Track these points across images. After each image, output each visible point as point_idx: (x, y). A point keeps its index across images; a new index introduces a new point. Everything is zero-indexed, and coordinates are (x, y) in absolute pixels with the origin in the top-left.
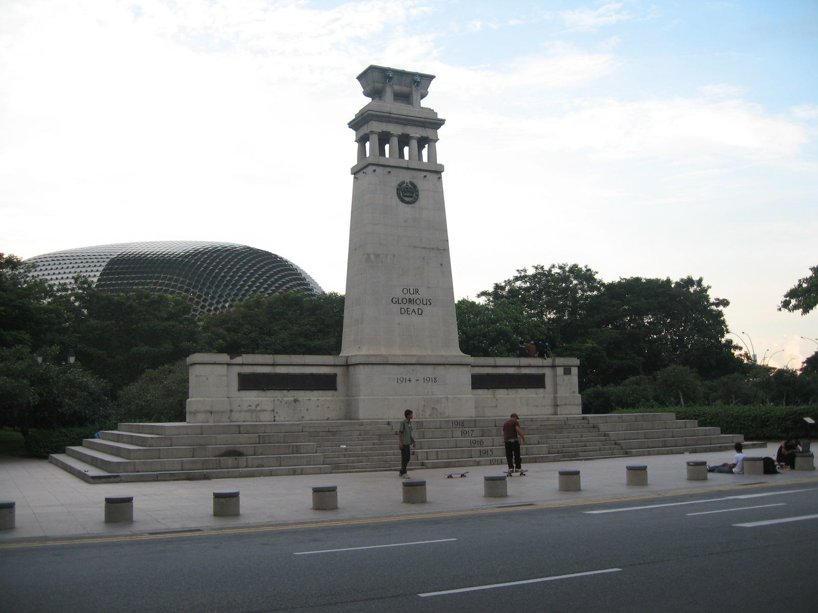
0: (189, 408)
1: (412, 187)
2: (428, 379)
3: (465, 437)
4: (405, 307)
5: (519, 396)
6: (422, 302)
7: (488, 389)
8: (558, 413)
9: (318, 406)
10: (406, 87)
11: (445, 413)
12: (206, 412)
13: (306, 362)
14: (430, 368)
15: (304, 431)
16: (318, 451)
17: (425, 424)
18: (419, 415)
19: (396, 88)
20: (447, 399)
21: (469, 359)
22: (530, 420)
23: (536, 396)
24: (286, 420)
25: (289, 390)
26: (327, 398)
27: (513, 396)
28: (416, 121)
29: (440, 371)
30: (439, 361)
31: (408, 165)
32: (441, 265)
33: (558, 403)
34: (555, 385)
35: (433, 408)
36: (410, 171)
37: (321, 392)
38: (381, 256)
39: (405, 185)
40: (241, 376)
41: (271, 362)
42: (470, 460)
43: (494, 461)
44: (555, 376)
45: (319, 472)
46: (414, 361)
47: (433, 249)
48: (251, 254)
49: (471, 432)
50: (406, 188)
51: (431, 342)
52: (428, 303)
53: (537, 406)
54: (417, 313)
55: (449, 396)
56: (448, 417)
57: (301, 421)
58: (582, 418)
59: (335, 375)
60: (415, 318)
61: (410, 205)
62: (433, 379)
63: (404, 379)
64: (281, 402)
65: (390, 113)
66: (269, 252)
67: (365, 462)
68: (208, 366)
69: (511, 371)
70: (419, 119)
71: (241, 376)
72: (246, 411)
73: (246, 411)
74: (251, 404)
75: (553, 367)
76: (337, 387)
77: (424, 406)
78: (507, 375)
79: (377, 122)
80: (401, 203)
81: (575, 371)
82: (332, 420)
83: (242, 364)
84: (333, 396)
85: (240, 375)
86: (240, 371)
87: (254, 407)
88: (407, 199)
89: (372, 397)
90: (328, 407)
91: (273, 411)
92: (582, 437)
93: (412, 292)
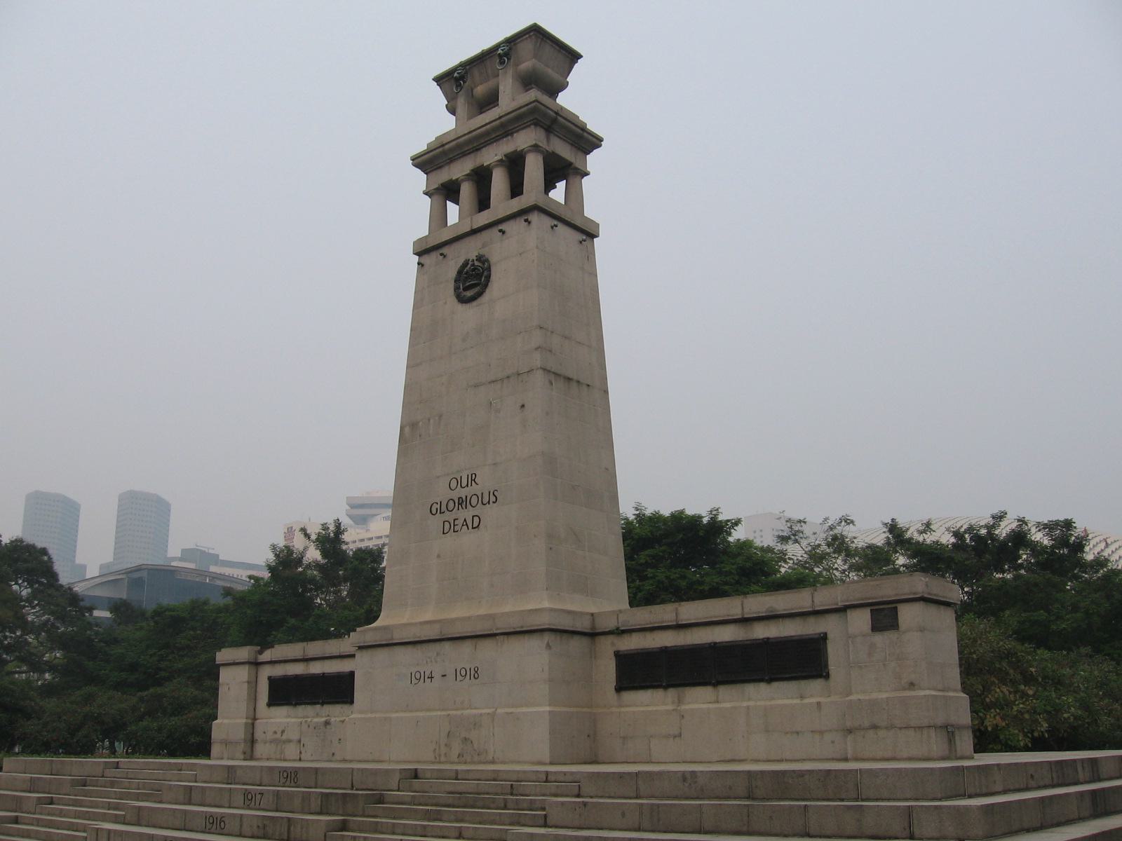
0: (215, 734)
4: (449, 516)
5: (745, 704)
11: (486, 752)
14: (467, 647)
18: (440, 756)
22: (453, 775)
25: (322, 704)
28: (487, 133)
29: (487, 650)
30: (480, 628)
32: (523, 406)
35: (465, 739)
38: (421, 423)
40: (273, 682)
47: (508, 377)
49: (258, 797)
53: (798, 733)
56: (493, 762)
60: (467, 539)
61: (474, 303)
62: (473, 672)
63: (422, 674)
65: (443, 145)
69: (725, 635)
70: (488, 126)
71: (273, 682)
73: (271, 742)
78: (714, 647)
87: (278, 735)
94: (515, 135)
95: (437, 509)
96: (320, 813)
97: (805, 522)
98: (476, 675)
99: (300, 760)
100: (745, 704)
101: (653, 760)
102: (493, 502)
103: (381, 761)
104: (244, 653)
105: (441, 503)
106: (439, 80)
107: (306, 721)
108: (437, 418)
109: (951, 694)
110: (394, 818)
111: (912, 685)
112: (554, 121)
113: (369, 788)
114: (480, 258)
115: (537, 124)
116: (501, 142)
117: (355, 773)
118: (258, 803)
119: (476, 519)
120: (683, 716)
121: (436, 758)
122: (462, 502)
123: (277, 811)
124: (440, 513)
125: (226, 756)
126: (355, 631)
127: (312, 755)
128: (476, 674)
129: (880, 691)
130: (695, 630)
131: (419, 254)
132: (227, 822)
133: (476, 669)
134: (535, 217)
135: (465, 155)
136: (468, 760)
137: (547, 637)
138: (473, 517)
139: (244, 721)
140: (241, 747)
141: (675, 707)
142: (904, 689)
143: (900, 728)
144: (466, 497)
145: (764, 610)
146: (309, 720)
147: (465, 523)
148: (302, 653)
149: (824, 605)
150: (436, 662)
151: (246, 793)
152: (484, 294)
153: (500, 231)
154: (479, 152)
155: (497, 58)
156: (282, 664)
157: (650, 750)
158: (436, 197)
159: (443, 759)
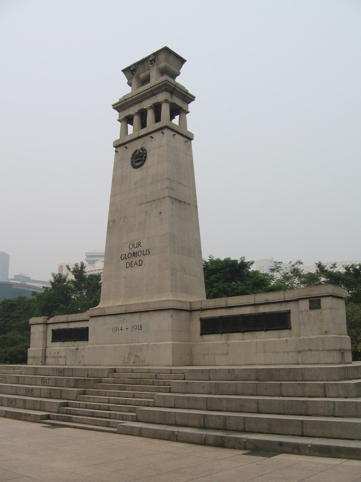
0: (29, 354)
2: (135, 328)
4: (129, 260)
5: (255, 340)
7: (222, 333)
13: (83, 318)
14: (137, 316)
18: (125, 363)
23: (278, 339)
25: (75, 341)
28: (145, 94)
32: (161, 213)
36: (142, 138)
38: (117, 220)
40: (54, 332)
41: (65, 320)
47: (154, 200)
49: (48, 380)
52: (148, 253)
56: (148, 365)
60: (137, 270)
61: (140, 168)
62: (139, 327)
64: (69, 350)
65: (126, 100)
70: (146, 91)
71: (54, 332)
73: (53, 357)
78: (243, 316)
80: (134, 169)
87: (56, 355)
88: (137, 164)
94: (157, 95)
96: (74, 387)
97: (282, 263)
98: (141, 328)
99: (66, 365)
100: (255, 340)
102: (148, 254)
103: (100, 365)
104: (41, 319)
105: (125, 254)
106: (124, 71)
108: (124, 218)
109: (343, 336)
110: (106, 389)
111: (326, 332)
112: (174, 89)
113: (95, 376)
114: (142, 149)
115: (167, 90)
116: (151, 98)
117: (89, 371)
118: (47, 383)
119: (141, 261)
120: (229, 346)
121: (124, 364)
122: (134, 254)
123: (56, 386)
124: (125, 259)
125: (34, 363)
126: (89, 310)
127: (71, 363)
128: (140, 328)
129: (313, 335)
130: (234, 309)
131: (116, 147)
132: (34, 391)
133: (141, 326)
134: (166, 131)
135: (136, 104)
136: (138, 365)
137: (171, 312)
139: (41, 348)
140: (40, 360)
143: (321, 351)
144: (136, 252)
146: (70, 348)
147: (136, 263)
149: (289, 298)
150: (124, 323)
151: (43, 379)
152: (144, 165)
153: (151, 137)
154: (142, 103)
155: (149, 61)
156: (58, 324)
157: (215, 360)
158: (123, 122)
159: (127, 364)
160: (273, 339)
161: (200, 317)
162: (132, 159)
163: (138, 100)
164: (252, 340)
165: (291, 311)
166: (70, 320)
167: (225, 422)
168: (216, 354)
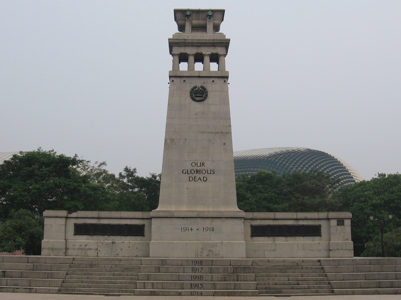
1: (202, 89)
2: (207, 229)
3: (195, 273)
4: (193, 176)
5: (296, 242)
6: (207, 172)
8: (331, 256)
9: (129, 247)
10: (203, 20)
11: (219, 254)
12: (49, 249)
15: (73, 263)
16: (256, 280)
17: (168, 262)
18: (198, 255)
19: (195, 22)
20: (222, 243)
21: (243, 214)
22: (267, 261)
23: (313, 242)
24: (106, 255)
25: (109, 236)
26: (136, 242)
27: (291, 242)
29: (217, 223)
30: (215, 215)
31: (199, 75)
33: (331, 249)
34: (329, 234)
36: (201, 78)
37: (132, 237)
38: (176, 140)
39: (197, 88)
40: (76, 226)
42: (172, 291)
43: (195, 293)
44: (329, 227)
45: (49, 293)
46: (194, 215)
47: (218, 133)
48: (310, 154)
49: (201, 269)
50: (197, 91)
51: (214, 201)
52: (212, 172)
53: (313, 250)
54: (202, 180)
55: (224, 242)
56: (222, 257)
57: (116, 257)
58: (318, 261)
59: (144, 226)
60: (201, 184)
61: (200, 103)
62: (211, 229)
64: (103, 244)
65: (185, 40)
66: (326, 152)
67: (93, 288)
68: (52, 219)
70: (208, 41)
71: (76, 226)
72: (78, 249)
73: (78, 249)
74: (82, 244)
75: (328, 219)
76: (145, 234)
77: (202, 249)
78: (286, 226)
79: (177, 47)
81: (348, 223)
82: (139, 257)
83: (77, 218)
84: (141, 240)
85: (75, 225)
86: (75, 222)
87: (83, 247)
88: (198, 99)
89: (160, 241)
90: (137, 248)
91: (97, 249)
92: (302, 276)
93: (199, 165)
94: (216, 47)
95: (186, 172)
100: (296, 242)
101: (265, 257)
105: (188, 170)
106: (176, 11)
107: (100, 242)
108: (184, 140)
116: (210, 47)
118: (200, 271)
120: (276, 245)
121: (196, 256)
124: (187, 173)
126: (152, 211)
128: (213, 229)
129: (339, 241)
138: (204, 177)
141: (273, 242)
142: (345, 240)
143: (345, 250)
144: (200, 170)
145: (304, 217)
148: (98, 215)
149: (321, 217)
152: (205, 101)
154: (199, 48)
160: (310, 242)
161: (251, 224)
162: (191, 92)
163: (197, 45)
164: (294, 242)
165: (322, 226)
166: (122, 216)
167: (392, 284)
168: (265, 250)
